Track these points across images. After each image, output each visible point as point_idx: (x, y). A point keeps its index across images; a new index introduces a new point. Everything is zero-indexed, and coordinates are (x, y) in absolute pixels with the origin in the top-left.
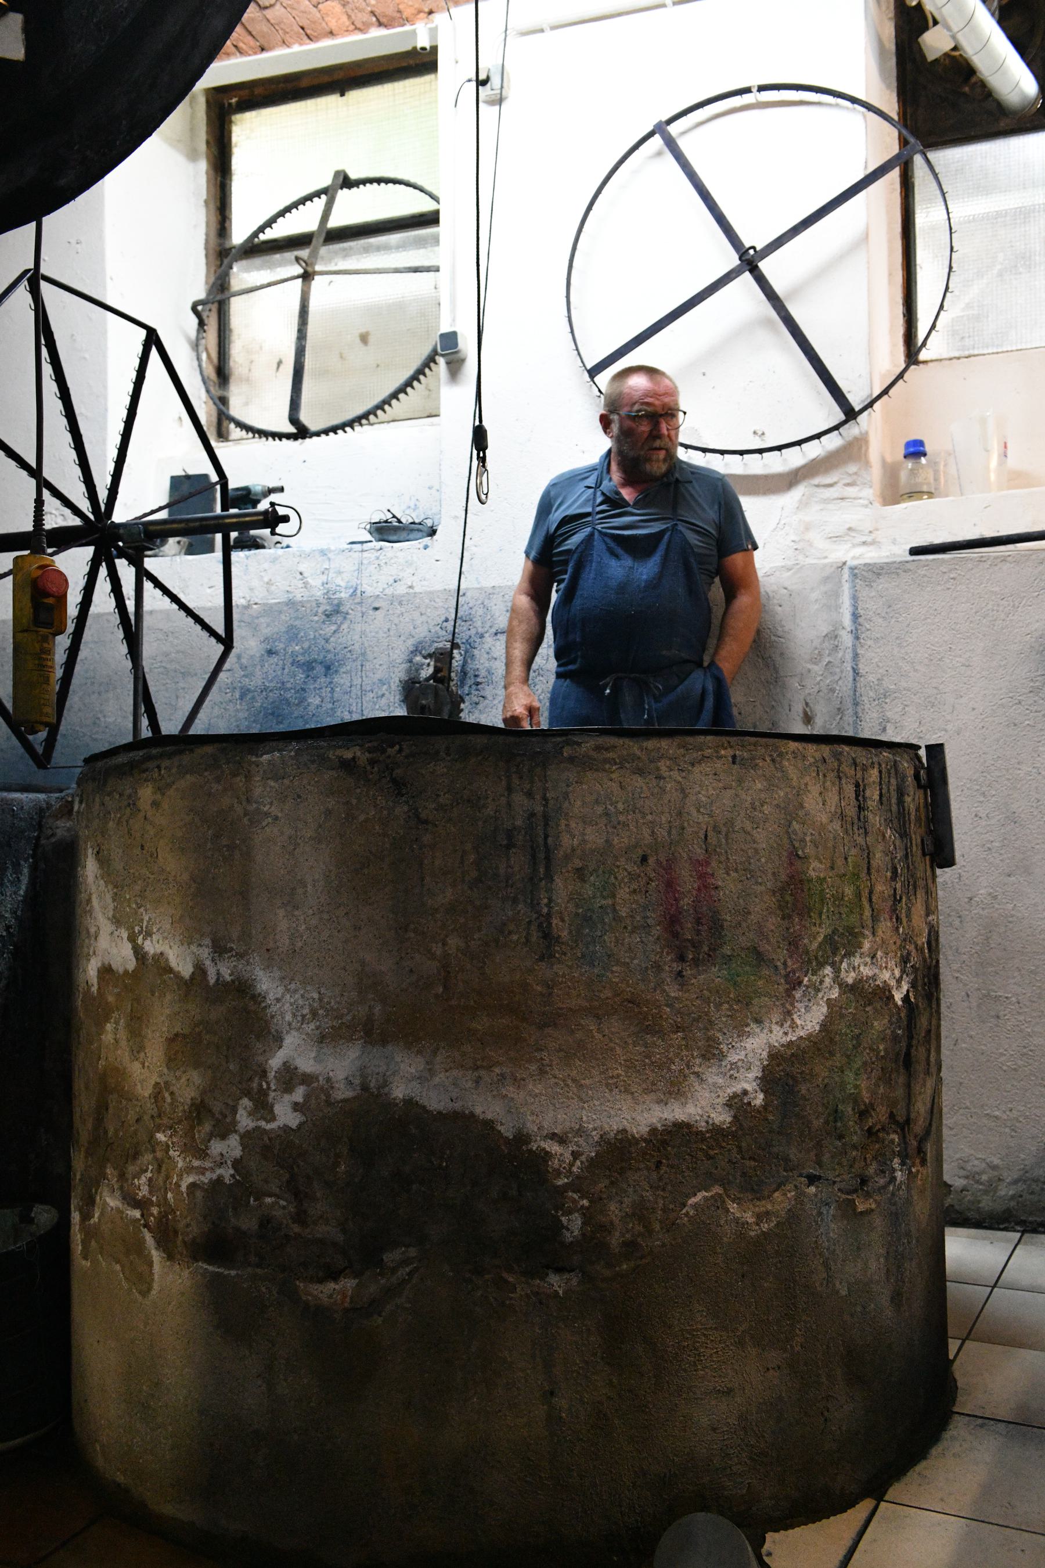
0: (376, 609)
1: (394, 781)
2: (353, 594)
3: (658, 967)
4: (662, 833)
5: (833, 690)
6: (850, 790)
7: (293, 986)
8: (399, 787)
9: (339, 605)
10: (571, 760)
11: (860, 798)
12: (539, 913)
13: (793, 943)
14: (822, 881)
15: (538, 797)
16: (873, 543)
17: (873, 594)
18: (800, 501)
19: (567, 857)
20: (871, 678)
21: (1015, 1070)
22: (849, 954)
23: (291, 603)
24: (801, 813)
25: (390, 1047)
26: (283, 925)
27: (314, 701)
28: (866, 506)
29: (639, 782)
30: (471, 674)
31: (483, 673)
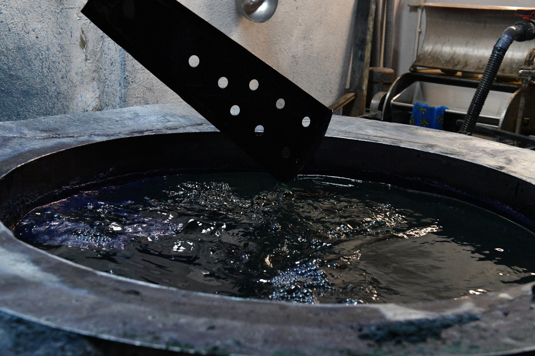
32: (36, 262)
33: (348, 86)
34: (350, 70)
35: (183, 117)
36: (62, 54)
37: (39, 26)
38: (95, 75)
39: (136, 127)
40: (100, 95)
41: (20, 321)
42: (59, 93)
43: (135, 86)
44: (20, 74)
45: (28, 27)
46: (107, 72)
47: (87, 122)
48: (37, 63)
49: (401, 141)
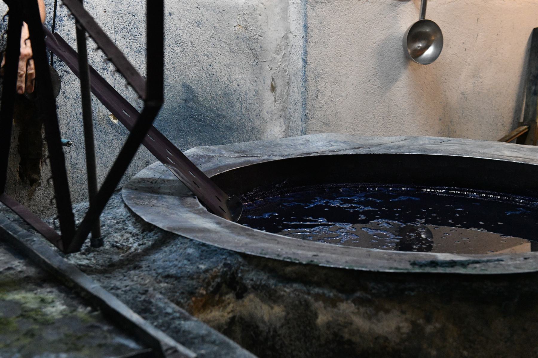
5: (285, 71)
17: (314, 14)
32: (218, 223)
33: (522, 120)
34: (524, 105)
35: (345, 142)
36: (256, 97)
37: (240, 76)
38: (282, 113)
39: (306, 150)
40: (285, 130)
41: (204, 245)
42: (253, 128)
43: (314, 121)
45: (232, 78)
46: (292, 111)
47: (268, 147)
48: (238, 105)
49: (533, 160)
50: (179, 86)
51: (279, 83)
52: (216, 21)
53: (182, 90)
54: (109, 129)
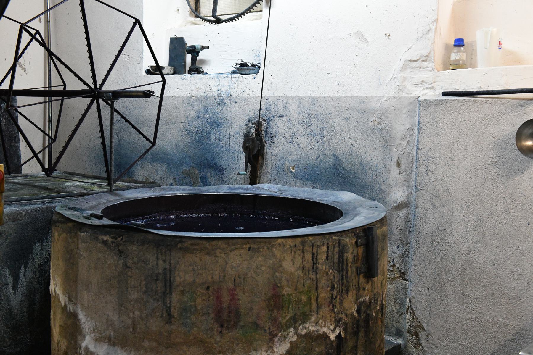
0: (236, 102)
1: (119, 250)
2: (228, 96)
3: (212, 329)
4: (216, 278)
5: (410, 153)
6: (309, 256)
7: (88, 319)
8: (121, 253)
9: (223, 100)
10: (180, 249)
11: (315, 260)
12: (166, 306)
13: (274, 320)
14: (289, 295)
15: (168, 262)
16: (433, 88)
18: (402, 68)
19: (178, 286)
20: (424, 151)
21: (473, 327)
22: (303, 323)
23: (206, 97)
24: (280, 269)
25: (116, 347)
26: (86, 296)
27: (213, 138)
28: (431, 71)
29: (207, 258)
30: (269, 132)
31: (274, 132)
44: (360, 176)
50: (331, 156)
51: (404, 161)
52: (359, 118)
53: (333, 158)
54: (289, 174)
